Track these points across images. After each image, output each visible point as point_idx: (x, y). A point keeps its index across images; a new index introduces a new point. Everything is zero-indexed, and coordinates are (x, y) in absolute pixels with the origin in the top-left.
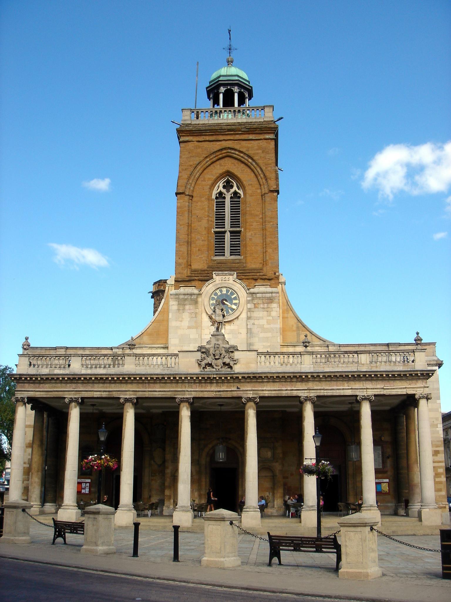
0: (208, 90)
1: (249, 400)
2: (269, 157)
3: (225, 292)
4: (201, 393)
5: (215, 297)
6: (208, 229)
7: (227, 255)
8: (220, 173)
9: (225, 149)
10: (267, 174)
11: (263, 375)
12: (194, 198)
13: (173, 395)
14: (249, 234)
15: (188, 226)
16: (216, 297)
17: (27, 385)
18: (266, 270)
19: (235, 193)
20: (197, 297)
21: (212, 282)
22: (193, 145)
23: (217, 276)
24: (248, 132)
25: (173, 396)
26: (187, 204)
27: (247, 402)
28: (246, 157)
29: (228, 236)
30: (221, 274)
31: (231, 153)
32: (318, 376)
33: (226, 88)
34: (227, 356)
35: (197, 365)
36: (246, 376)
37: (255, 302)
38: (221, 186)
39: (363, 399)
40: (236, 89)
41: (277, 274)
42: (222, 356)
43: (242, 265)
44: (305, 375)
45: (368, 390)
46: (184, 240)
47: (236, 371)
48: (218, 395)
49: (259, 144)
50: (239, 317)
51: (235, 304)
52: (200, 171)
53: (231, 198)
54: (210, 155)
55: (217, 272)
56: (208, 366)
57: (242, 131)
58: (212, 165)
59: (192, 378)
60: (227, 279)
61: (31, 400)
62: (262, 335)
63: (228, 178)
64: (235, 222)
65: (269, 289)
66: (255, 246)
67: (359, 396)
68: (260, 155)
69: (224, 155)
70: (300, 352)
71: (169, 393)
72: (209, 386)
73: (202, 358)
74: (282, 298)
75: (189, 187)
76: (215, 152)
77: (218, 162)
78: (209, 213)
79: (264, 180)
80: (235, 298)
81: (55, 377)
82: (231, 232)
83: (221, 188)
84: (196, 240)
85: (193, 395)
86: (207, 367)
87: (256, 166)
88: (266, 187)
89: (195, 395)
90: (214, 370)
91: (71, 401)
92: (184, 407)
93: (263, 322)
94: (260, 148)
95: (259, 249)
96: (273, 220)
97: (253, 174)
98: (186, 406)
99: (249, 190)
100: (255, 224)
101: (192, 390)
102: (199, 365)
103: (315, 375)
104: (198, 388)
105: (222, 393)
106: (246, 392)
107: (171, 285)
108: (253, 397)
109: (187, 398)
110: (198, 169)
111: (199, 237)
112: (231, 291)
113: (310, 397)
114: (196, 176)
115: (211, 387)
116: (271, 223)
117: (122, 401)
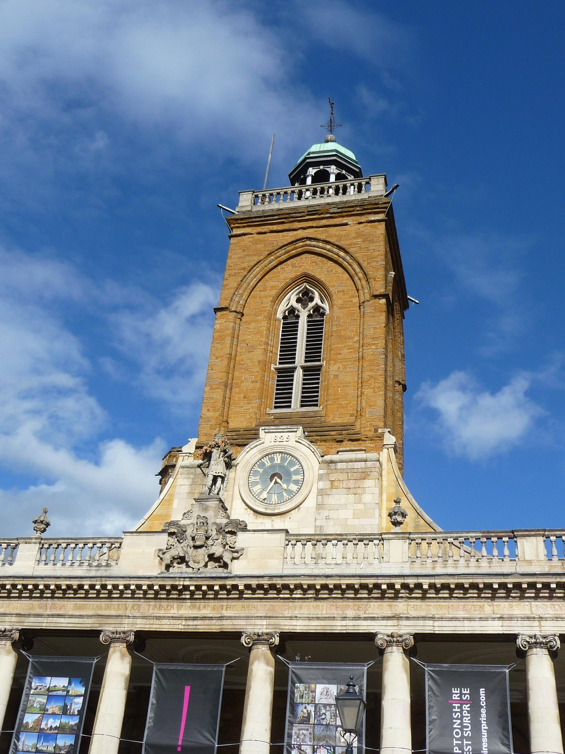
1: (259, 639)
2: (374, 248)
3: (279, 462)
5: (260, 470)
6: (264, 365)
10: (370, 273)
12: (244, 317)
13: (97, 625)
15: (230, 359)
16: (261, 470)
19: (317, 309)
21: (257, 444)
22: (251, 239)
26: (232, 324)
27: (253, 644)
28: (336, 250)
29: (298, 375)
30: (274, 431)
31: (310, 246)
33: (318, 169)
34: (220, 541)
39: (532, 646)
40: (333, 170)
41: (380, 431)
44: (388, 581)
45: (543, 623)
46: (220, 381)
47: (235, 572)
49: (359, 229)
50: (301, 506)
51: (296, 482)
52: (259, 276)
53: (309, 316)
55: (267, 428)
56: (178, 563)
57: (331, 213)
58: (279, 267)
60: (285, 439)
63: (306, 287)
66: (343, 386)
67: (520, 637)
68: (359, 245)
70: (381, 534)
74: (388, 473)
75: (237, 299)
77: (289, 262)
78: (267, 338)
79: (364, 282)
80: (296, 472)
82: (305, 369)
83: (293, 303)
84: (242, 382)
85: (138, 626)
86: (175, 564)
87: (351, 261)
88: (366, 291)
89: (142, 626)
90: (190, 570)
92: (114, 652)
95: (352, 391)
96: (376, 342)
98: (121, 651)
99: (338, 300)
100: (346, 351)
105: (200, 622)
106: (253, 622)
107: (188, 455)
108: (267, 634)
109: (124, 633)
110: (254, 273)
111: (247, 376)
112: (289, 459)
114: (251, 284)
115: (179, 608)
116: (373, 347)
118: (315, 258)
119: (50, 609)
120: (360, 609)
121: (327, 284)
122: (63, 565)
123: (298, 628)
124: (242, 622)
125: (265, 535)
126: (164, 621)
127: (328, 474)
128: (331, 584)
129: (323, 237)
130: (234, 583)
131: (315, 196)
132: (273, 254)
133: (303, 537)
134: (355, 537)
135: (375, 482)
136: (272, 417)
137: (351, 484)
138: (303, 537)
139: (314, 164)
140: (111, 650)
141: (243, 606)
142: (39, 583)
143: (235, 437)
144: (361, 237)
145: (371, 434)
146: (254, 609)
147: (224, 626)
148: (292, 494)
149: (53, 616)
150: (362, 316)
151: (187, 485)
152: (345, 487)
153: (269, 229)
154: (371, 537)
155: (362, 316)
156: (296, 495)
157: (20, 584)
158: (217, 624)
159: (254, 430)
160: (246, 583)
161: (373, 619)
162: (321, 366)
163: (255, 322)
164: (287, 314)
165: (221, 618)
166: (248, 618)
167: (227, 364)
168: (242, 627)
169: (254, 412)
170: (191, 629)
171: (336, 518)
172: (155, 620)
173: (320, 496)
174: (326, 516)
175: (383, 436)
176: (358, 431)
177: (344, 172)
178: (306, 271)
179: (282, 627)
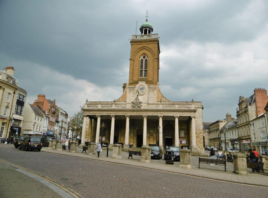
1: (145, 116)
6: (138, 70)
7: (143, 77)
9: (143, 47)
17: (87, 112)
19: (146, 59)
29: (144, 71)
32: (164, 110)
38: (142, 57)
40: (148, 29)
47: (141, 109)
48: (136, 115)
51: (145, 90)
59: (130, 110)
61: (88, 116)
62: (152, 99)
64: (146, 67)
65: (154, 86)
76: (141, 48)
80: (145, 89)
81: (94, 110)
82: (145, 70)
83: (142, 58)
91: (98, 116)
93: (152, 95)
97: (151, 54)
103: (163, 110)
117: (111, 116)
139: (144, 28)
150: (154, 62)
155: (154, 62)
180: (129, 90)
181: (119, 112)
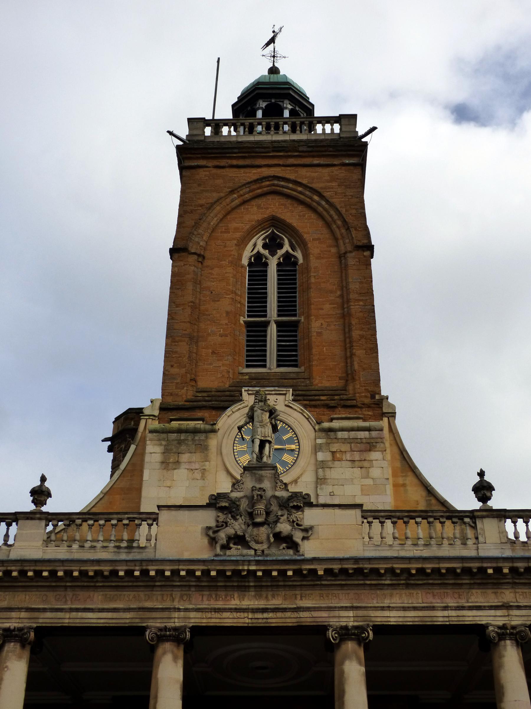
0: (235, 108)
2: (351, 194)
4: (214, 615)
8: (258, 220)
11: (382, 566)
13: (137, 620)
14: (315, 325)
18: (354, 389)
20: (207, 438)
21: (239, 407)
22: (207, 173)
23: (250, 396)
24: (311, 154)
25: (137, 623)
28: (307, 193)
29: (272, 331)
31: (278, 186)
33: (269, 103)
34: (285, 517)
35: (206, 541)
36: (336, 567)
37: (335, 447)
38: (260, 243)
41: (377, 397)
42: (272, 518)
43: (303, 382)
44: (494, 565)
49: (333, 172)
52: (220, 216)
53: (279, 265)
54: (240, 187)
55: (250, 388)
56: (234, 544)
63: (273, 232)
68: (334, 190)
69: (265, 189)
71: (128, 615)
72: (236, 595)
73: (220, 524)
74: (391, 445)
76: (249, 183)
77: (254, 203)
79: (343, 231)
82: (278, 324)
84: (209, 335)
85: (193, 621)
86: (231, 545)
87: (327, 206)
89: (197, 620)
90: (252, 552)
92: (164, 653)
94: (333, 179)
99: (314, 249)
100: (327, 306)
101: (191, 606)
102: (213, 541)
104: (207, 602)
105: (271, 615)
106: (336, 613)
110: (215, 211)
113: (513, 627)
115: (242, 598)
116: (361, 303)
118: (283, 200)
119: (71, 601)
120: (460, 596)
121: (301, 230)
122: (82, 547)
123: (392, 620)
124: (324, 614)
125: (338, 511)
126: (226, 615)
127: (328, 444)
128: (428, 568)
129: (292, 177)
130: (312, 567)
131: (269, 132)
132: (236, 191)
133: (382, 514)
134: (442, 514)
135: (383, 454)
136: (247, 377)
137: (357, 456)
138: (382, 514)
139: (264, 97)
140: (160, 651)
141: (322, 595)
142: (58, 568)
143: (207, 398)
144: (336, 181)
145: (367, 401)
146: (335, 598)
147: (301, 619)
148: (288, 466)
149: (77, 610)
151: (159, 453)
152: (348, 459)
153: (227, 163)
154: (461, 514)
155: (343, 268)
156: (292, 468)
157: (30, 570)
158: (292, 616)
159: (228, 391)
160: (326, 567)
161: (479, 608)
162: (298, 322)
163: (218, 268)
164: (253, 261)
165: (298, 609)
166: (330, 609)
167: (190, 313)
168: (324, 620)
169: (226, 371)
170: (261, 623)
171: (341, 494)
172: (213, 613)
173: (321, 469)
174: (330, 492)
175: (382, 403)
176: (351, 397)
177: (297, 109)
178: (274, 214)
179: (373, 619)
180: (166, 452)
181: (82, 594)
